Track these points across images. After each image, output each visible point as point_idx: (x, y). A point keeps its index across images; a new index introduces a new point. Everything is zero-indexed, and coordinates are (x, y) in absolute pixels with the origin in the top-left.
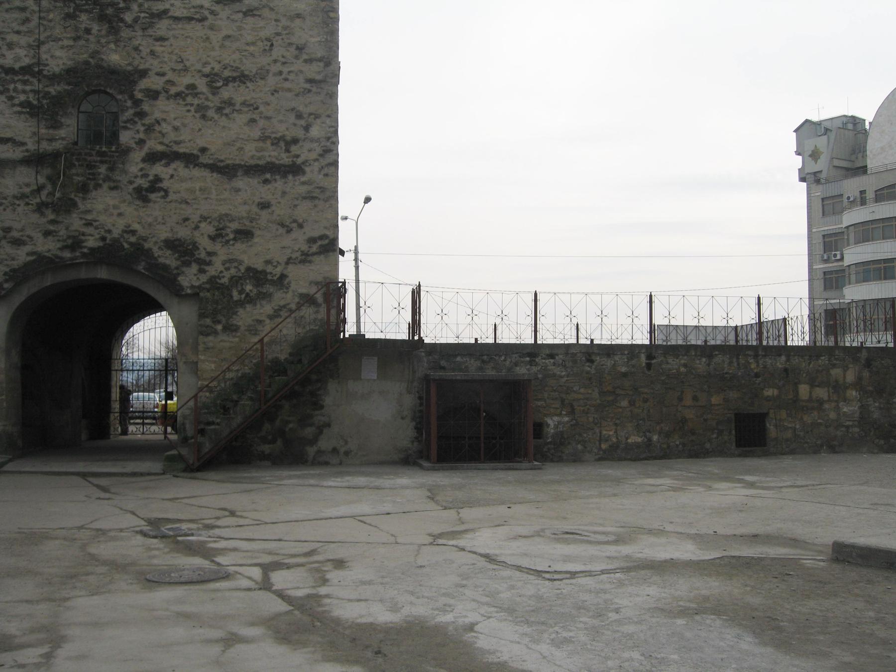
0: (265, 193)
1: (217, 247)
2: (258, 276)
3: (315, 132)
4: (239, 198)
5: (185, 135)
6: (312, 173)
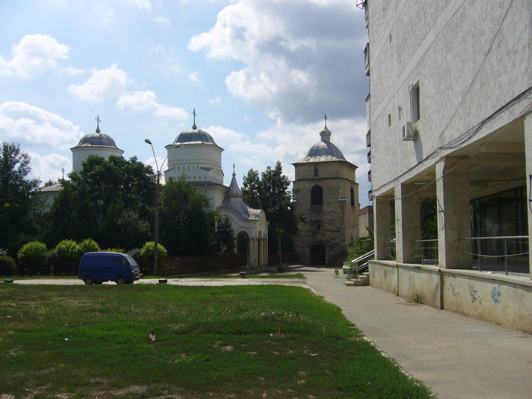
6: (342, 231)
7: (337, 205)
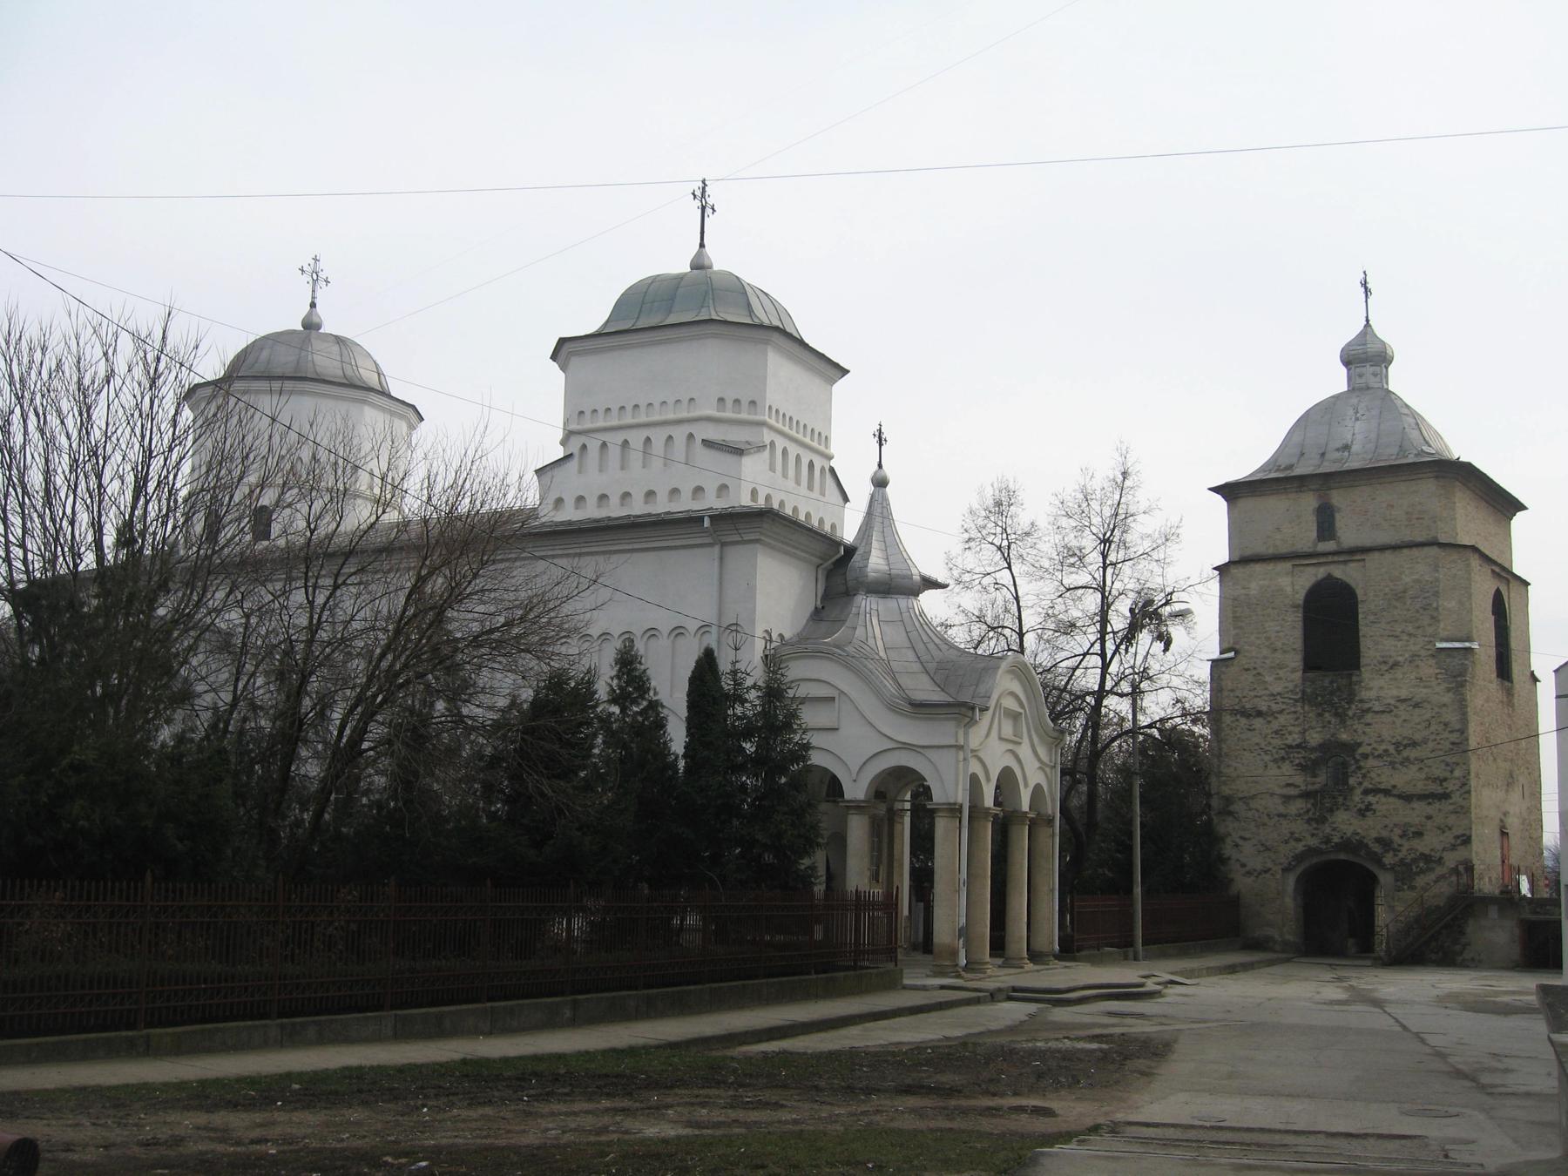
0: (1430, 810)
1: (1403, 841)
2: (1426, 858)
3: (1457, 773)
4: (1415, 814)
5: (1383, 778)
6: (1456, 798)
7: (1428, 669)
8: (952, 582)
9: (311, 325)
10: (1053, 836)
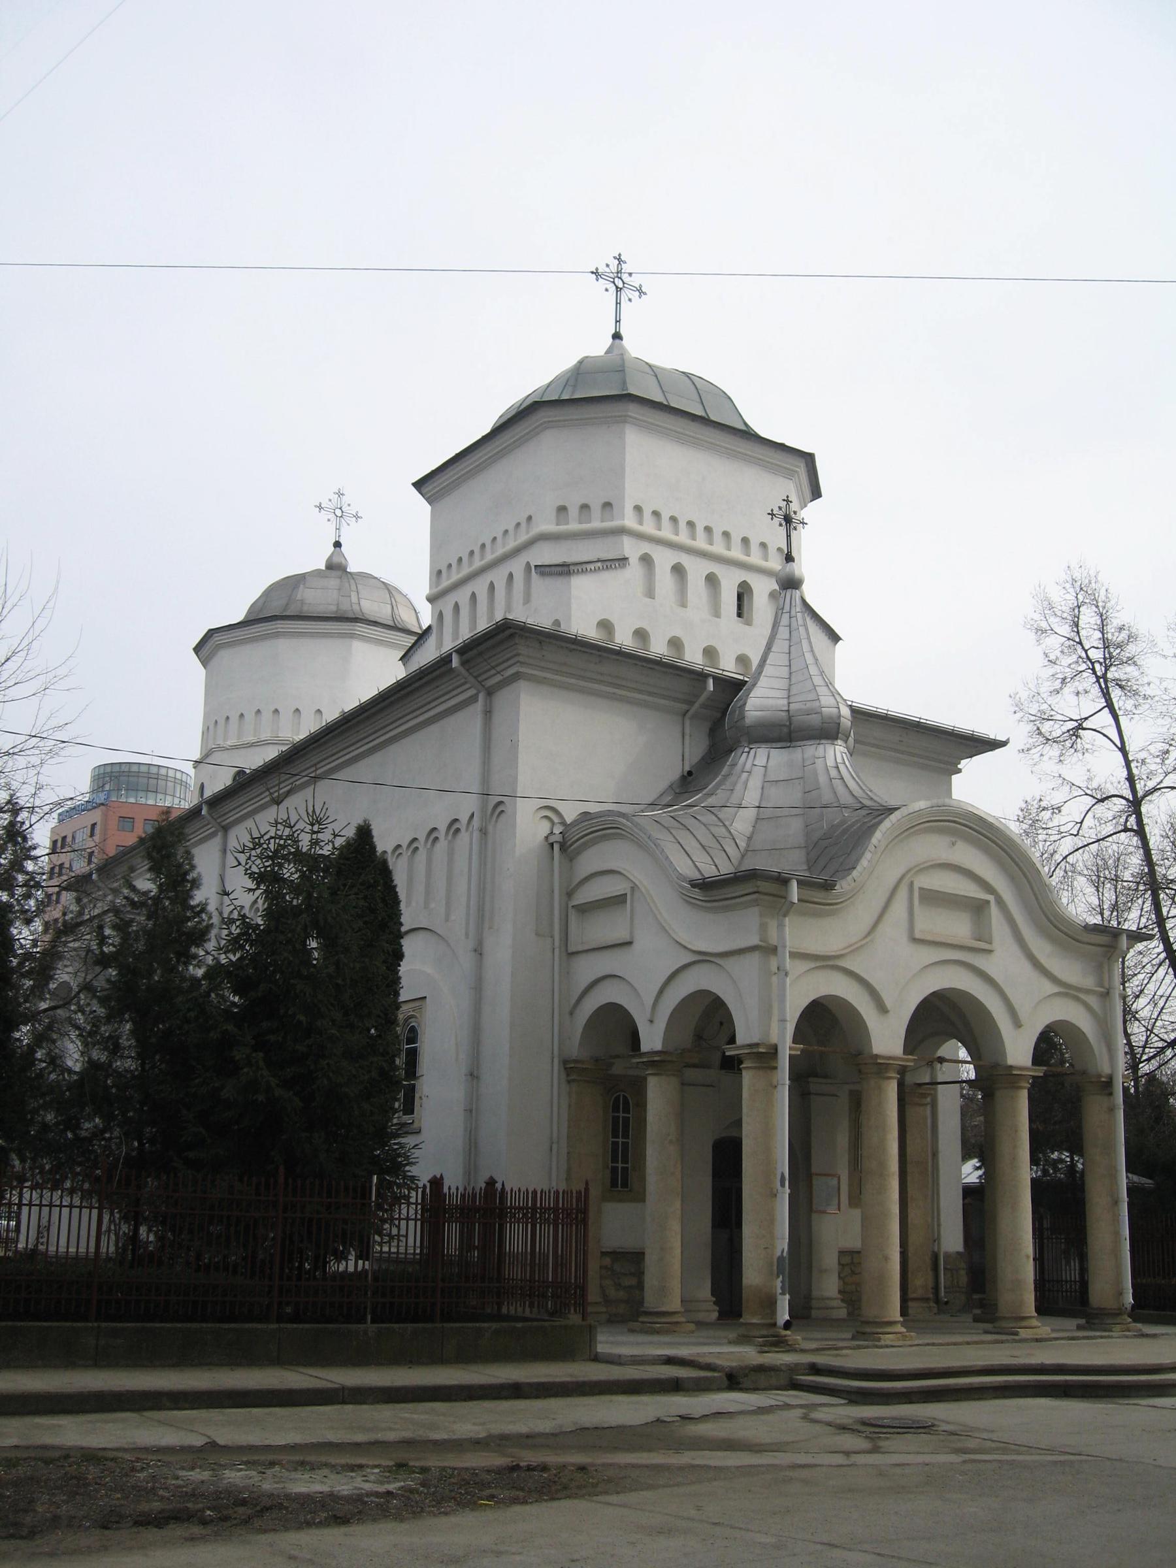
8: (1017, 732)
9: (336, 567)
10: (1112, 1110)
